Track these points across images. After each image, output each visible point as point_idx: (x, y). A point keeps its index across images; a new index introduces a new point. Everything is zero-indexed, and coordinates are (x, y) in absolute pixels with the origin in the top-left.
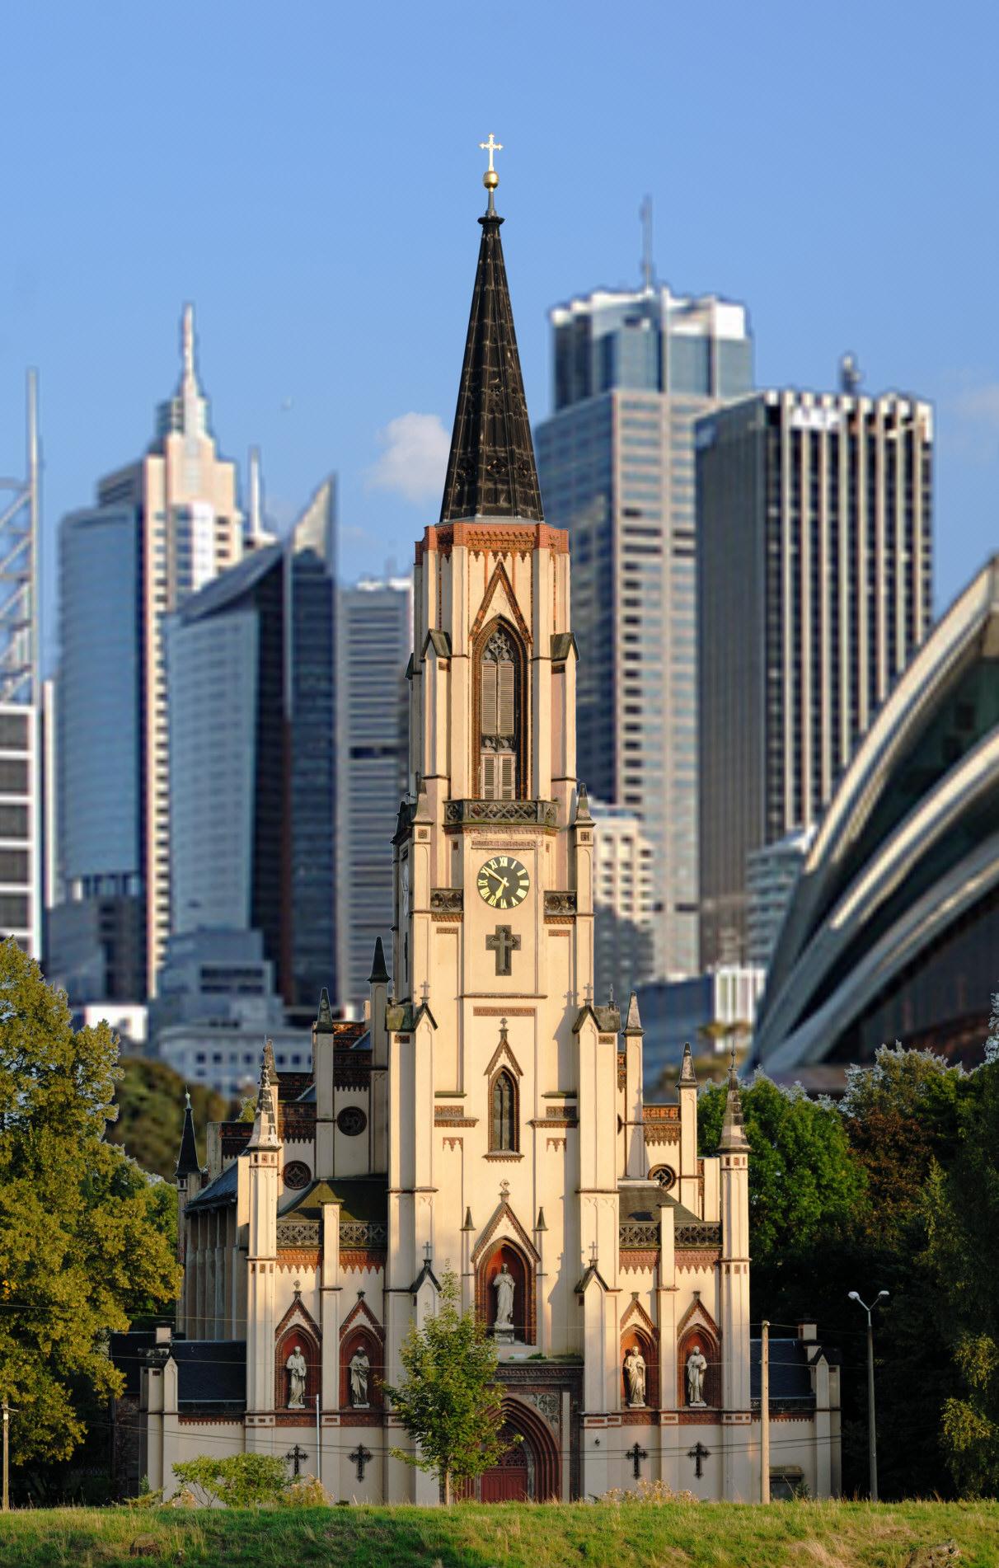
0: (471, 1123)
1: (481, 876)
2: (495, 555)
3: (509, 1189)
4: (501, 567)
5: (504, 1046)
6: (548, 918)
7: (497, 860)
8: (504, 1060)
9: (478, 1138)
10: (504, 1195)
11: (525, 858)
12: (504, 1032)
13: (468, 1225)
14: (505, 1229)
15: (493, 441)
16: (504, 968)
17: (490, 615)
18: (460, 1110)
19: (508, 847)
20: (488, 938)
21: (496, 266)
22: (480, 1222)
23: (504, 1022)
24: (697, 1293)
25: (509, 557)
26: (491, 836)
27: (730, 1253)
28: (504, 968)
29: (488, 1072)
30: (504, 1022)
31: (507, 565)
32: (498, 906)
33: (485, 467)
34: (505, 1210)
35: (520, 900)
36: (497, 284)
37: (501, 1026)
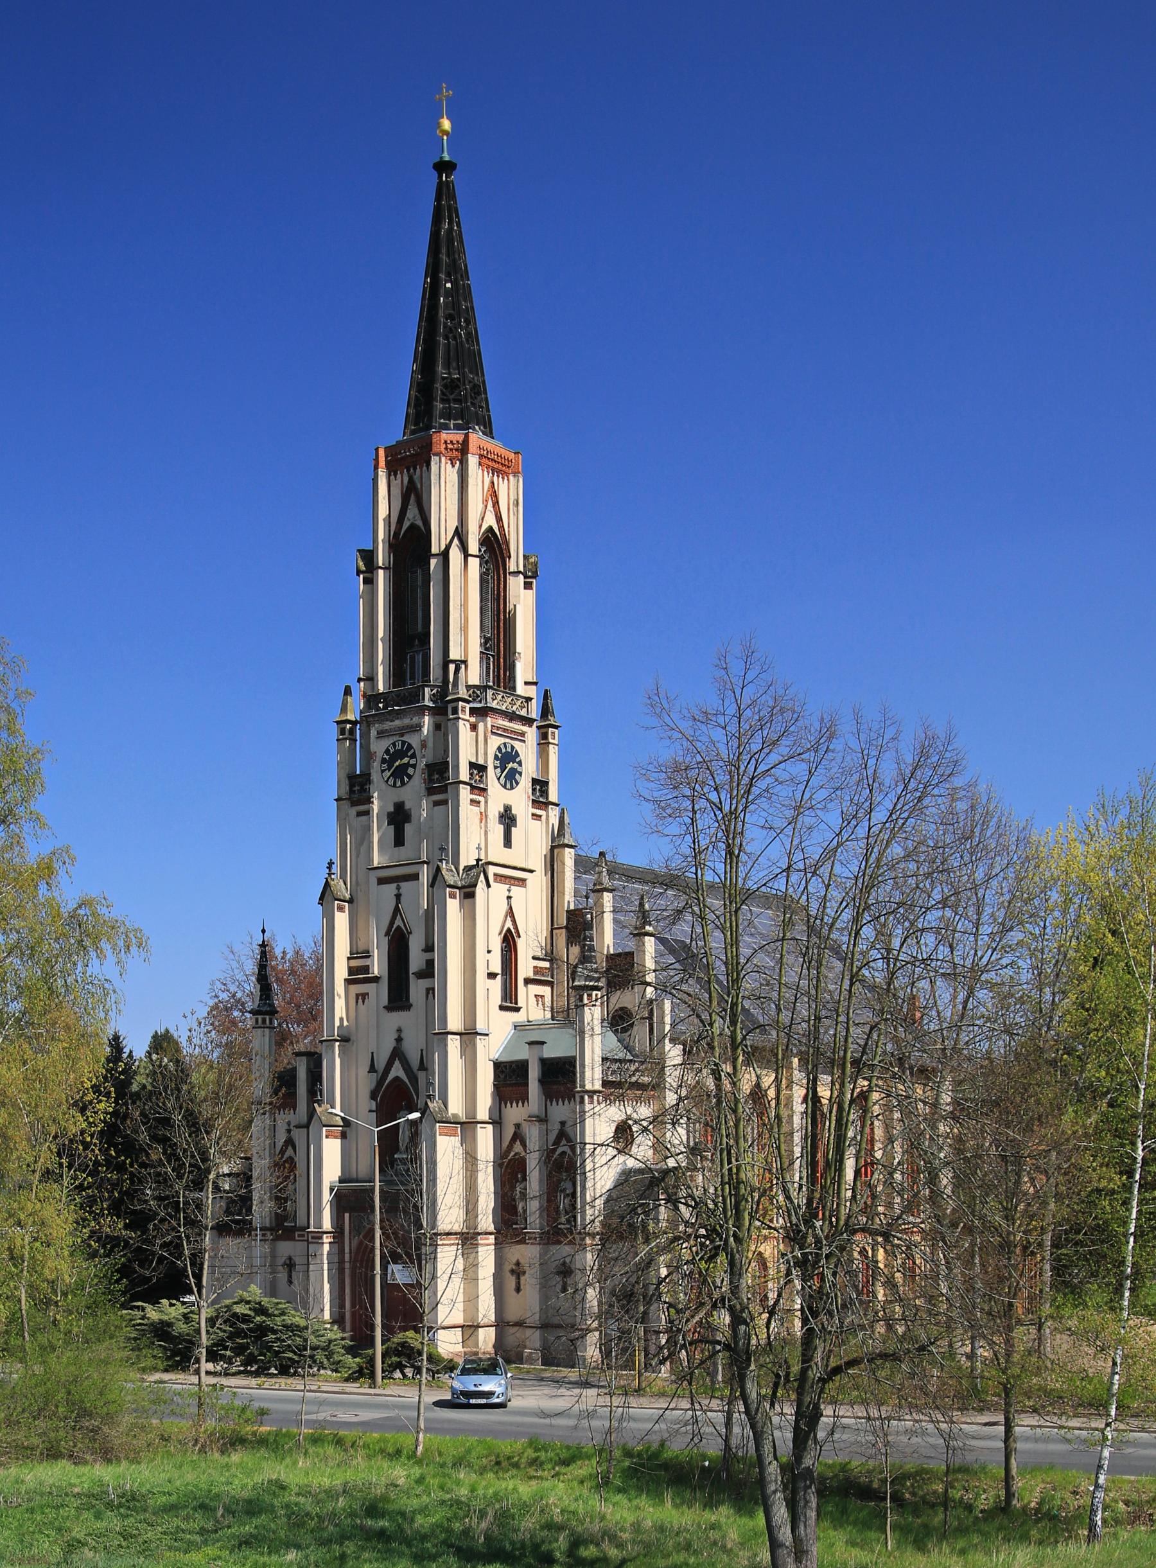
0: (376, 979)
1: (383, 761)
2: (408, 471)
3: (403, 1035)
4: (411, 480)
5: (397, 911)
6: (430, 791)
7: (394, 744)
8: (398, 922)
9: (380, 993)
10: (399, 1040)
11: (413, 740)
12: (398, 897)
13: (372, 1069)
14: (397, 1071)
15: (447, 365)
16: (399, 841)
17: (406, 524)
18: (366, 969)
19: (403, 731)
20: (389, 814)
21: (449, 207)
22: (381, 1065)
23: (398, 888)
24: (563, 1123)
25: (418, 470)
26: (388, 725)
27: (583, 1086)
28: (399, 841)
29: (387, 934)
30: (398, 888)
31: (416, 477)
32: (394, 786)
33: (438, 386)
34: (397, 1054)
35: (410, 777)
36: (450, 223)
37: (396, 892)
